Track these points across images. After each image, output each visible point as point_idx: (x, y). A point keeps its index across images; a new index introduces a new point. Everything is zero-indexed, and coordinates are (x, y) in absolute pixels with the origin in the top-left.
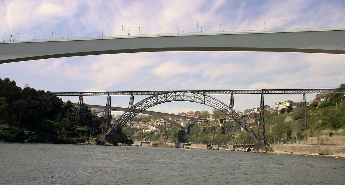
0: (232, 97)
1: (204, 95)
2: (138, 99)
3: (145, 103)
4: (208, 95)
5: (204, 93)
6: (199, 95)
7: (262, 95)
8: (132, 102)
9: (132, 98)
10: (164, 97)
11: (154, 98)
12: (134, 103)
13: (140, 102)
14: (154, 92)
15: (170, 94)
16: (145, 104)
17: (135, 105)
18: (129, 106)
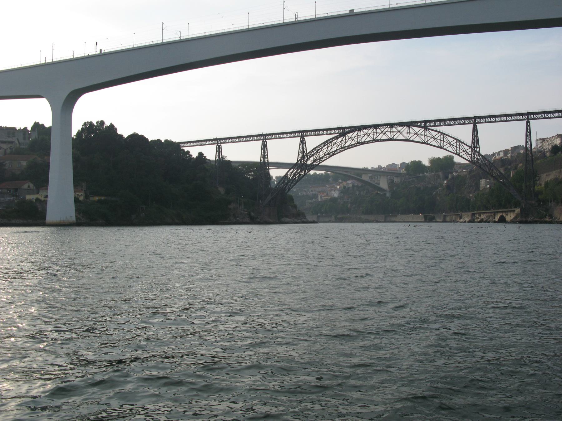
0: (475, 130)
1: (426, 128)
2: (312, 142)
3: (325, 149)
4: (433, 128)
5: (425, 124)
8: (303, 148)
9: (303, 142)
10: (356, 137)
11: (340, 139)
12: (306, 149)
13: (317, 147)
14: (339, 128)
15: (366, 131)
16: (325, 151)
17: (309, 153)
18: (298, 155)
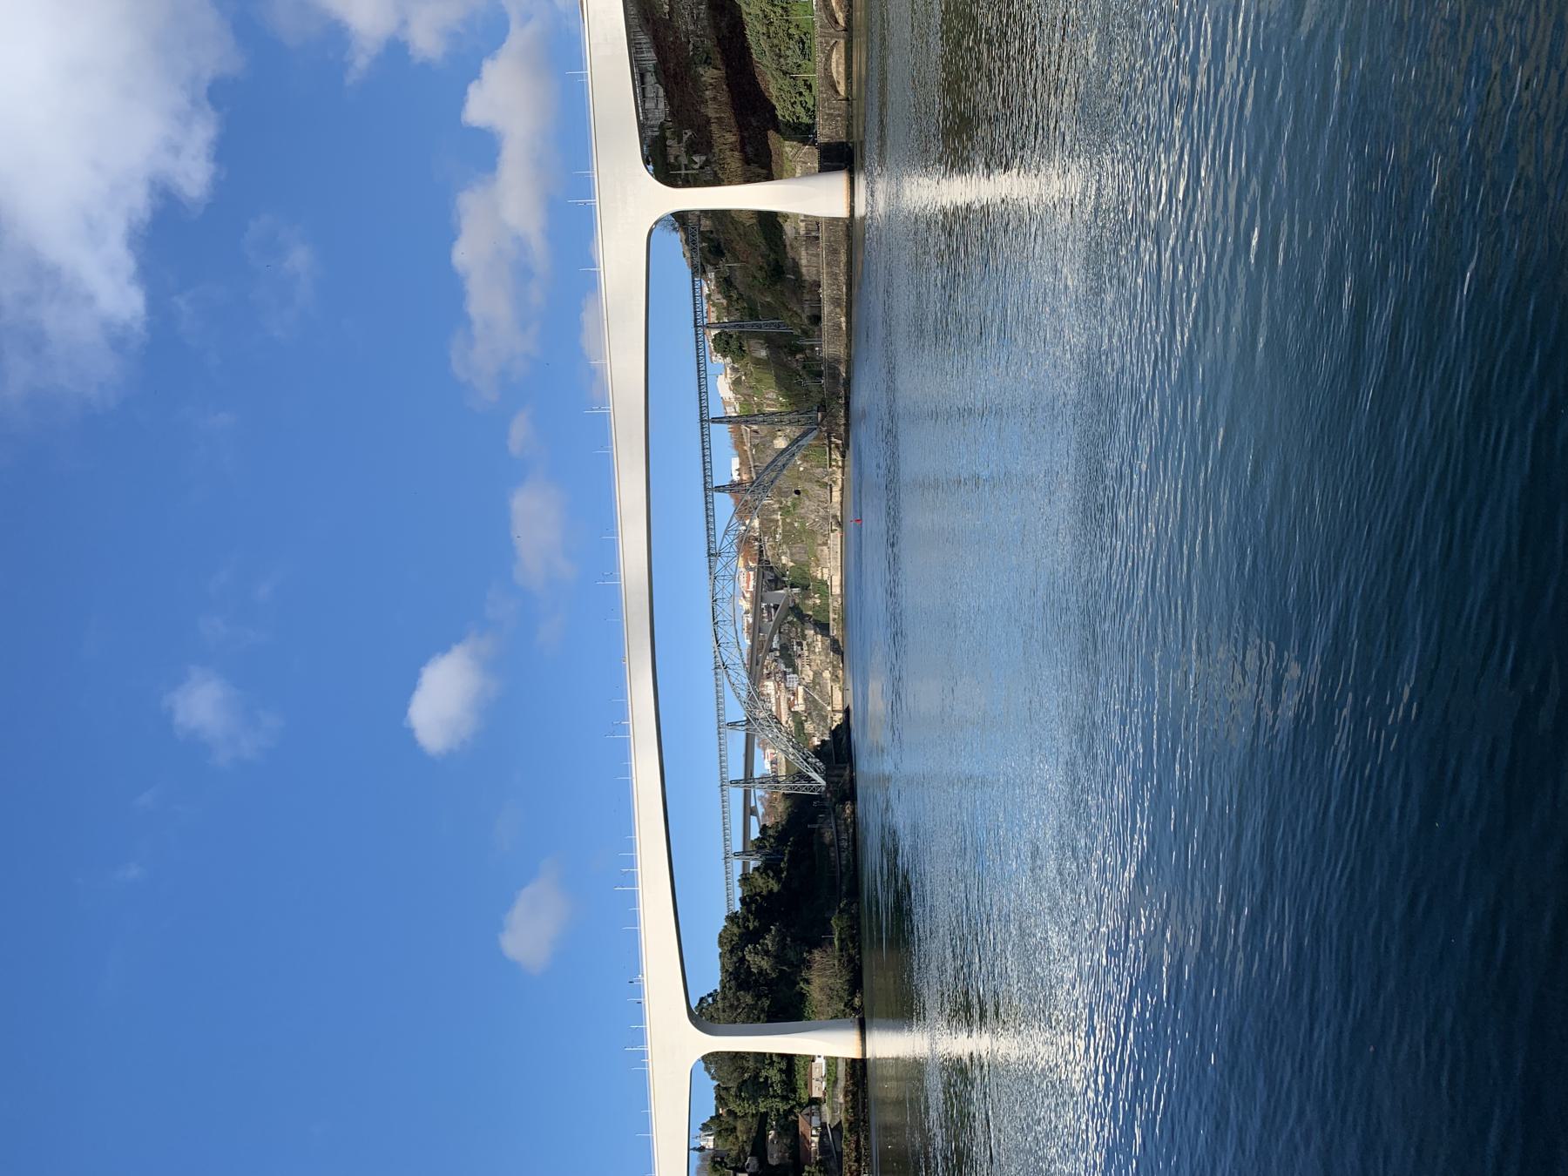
6: (719, 566)
7: (713, 422)
11: (730, 672)
